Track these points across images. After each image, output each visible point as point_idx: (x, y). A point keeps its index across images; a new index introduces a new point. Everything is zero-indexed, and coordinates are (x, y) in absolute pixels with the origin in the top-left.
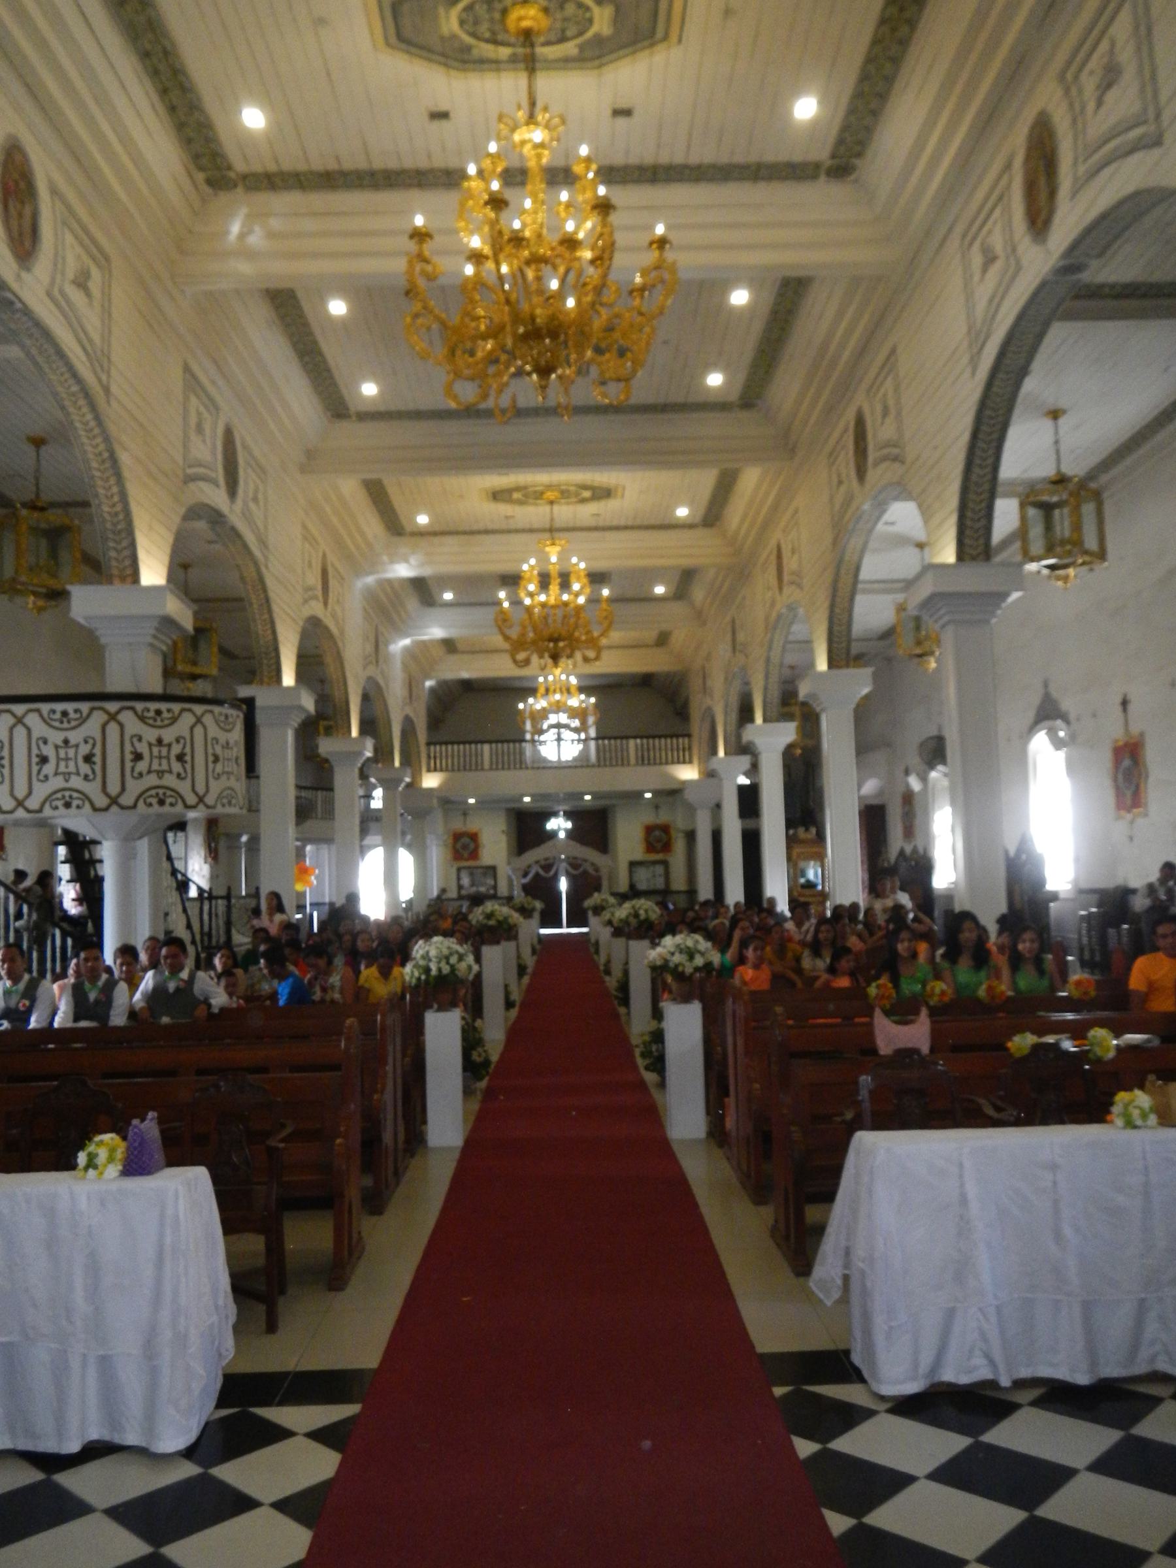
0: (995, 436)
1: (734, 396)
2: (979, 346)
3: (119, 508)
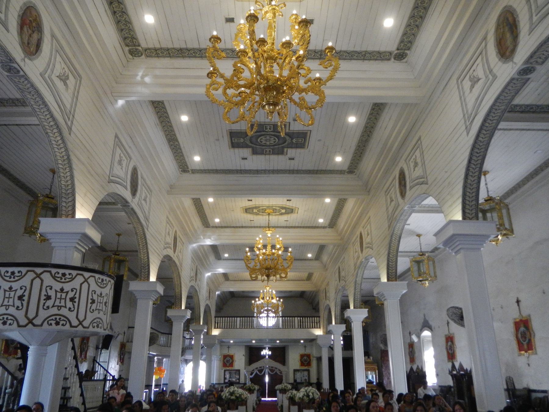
0: (479, 162)
1: (345, 168)
2: (471, 120)
3: (69, 182)
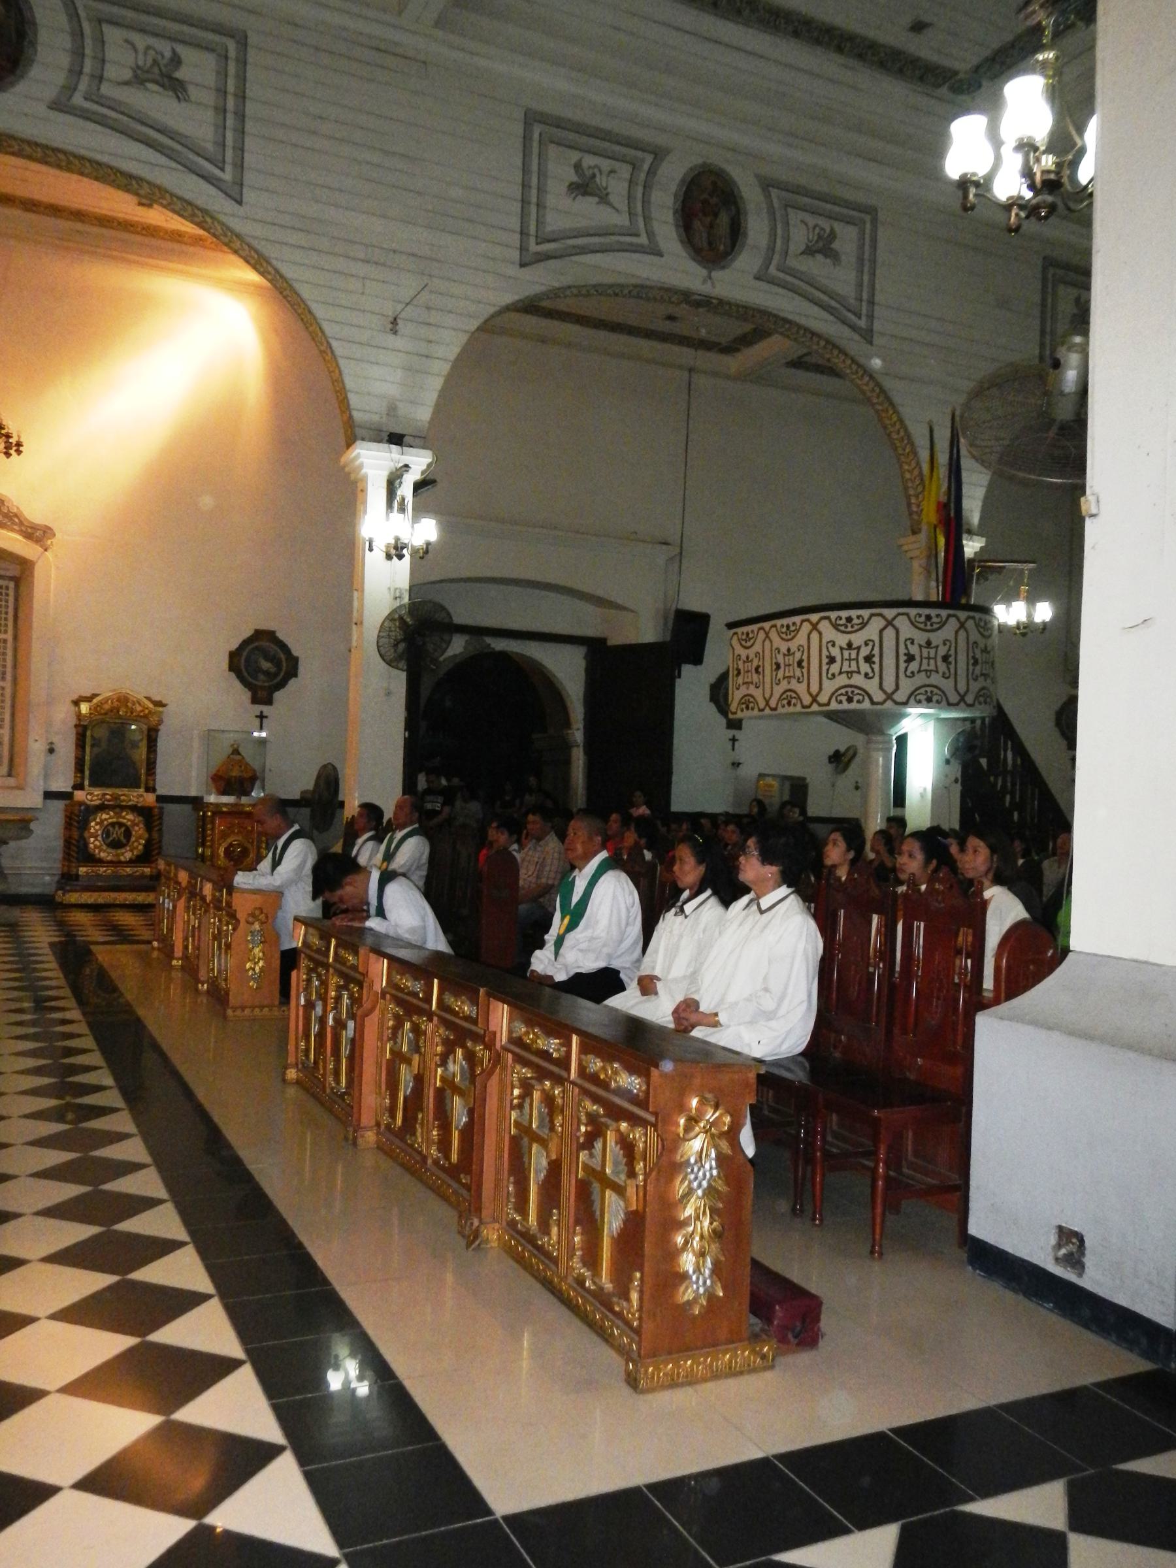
3: (902, 433)
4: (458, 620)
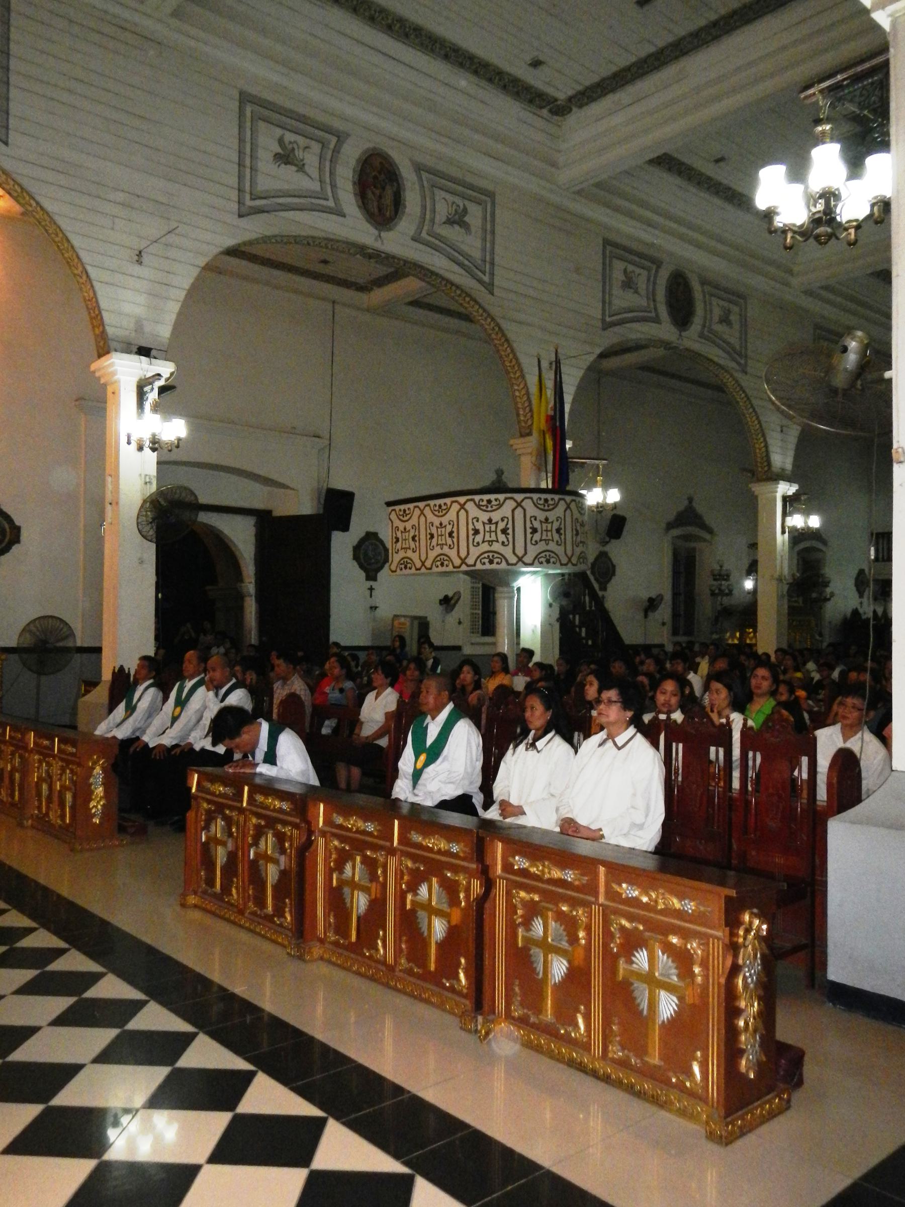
4: (203, 500)
